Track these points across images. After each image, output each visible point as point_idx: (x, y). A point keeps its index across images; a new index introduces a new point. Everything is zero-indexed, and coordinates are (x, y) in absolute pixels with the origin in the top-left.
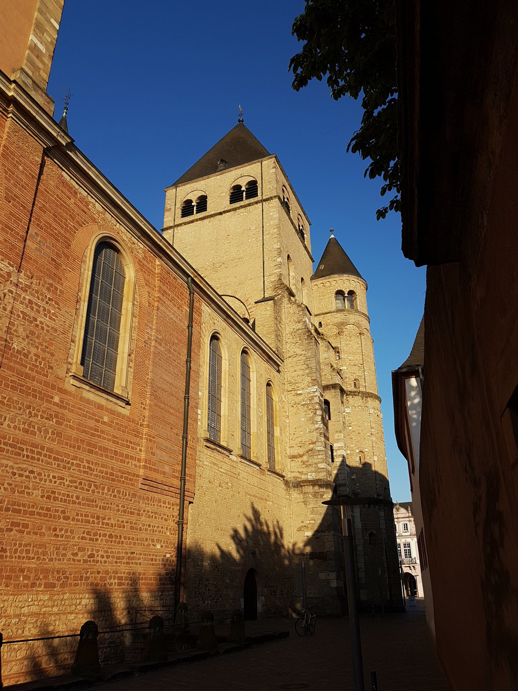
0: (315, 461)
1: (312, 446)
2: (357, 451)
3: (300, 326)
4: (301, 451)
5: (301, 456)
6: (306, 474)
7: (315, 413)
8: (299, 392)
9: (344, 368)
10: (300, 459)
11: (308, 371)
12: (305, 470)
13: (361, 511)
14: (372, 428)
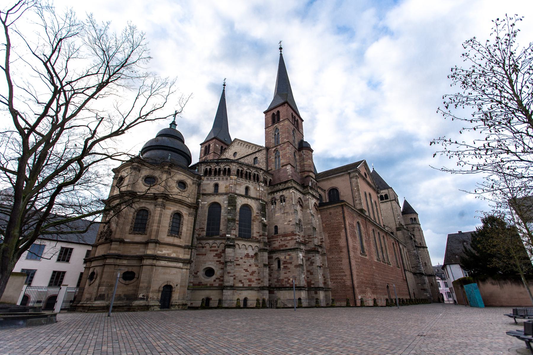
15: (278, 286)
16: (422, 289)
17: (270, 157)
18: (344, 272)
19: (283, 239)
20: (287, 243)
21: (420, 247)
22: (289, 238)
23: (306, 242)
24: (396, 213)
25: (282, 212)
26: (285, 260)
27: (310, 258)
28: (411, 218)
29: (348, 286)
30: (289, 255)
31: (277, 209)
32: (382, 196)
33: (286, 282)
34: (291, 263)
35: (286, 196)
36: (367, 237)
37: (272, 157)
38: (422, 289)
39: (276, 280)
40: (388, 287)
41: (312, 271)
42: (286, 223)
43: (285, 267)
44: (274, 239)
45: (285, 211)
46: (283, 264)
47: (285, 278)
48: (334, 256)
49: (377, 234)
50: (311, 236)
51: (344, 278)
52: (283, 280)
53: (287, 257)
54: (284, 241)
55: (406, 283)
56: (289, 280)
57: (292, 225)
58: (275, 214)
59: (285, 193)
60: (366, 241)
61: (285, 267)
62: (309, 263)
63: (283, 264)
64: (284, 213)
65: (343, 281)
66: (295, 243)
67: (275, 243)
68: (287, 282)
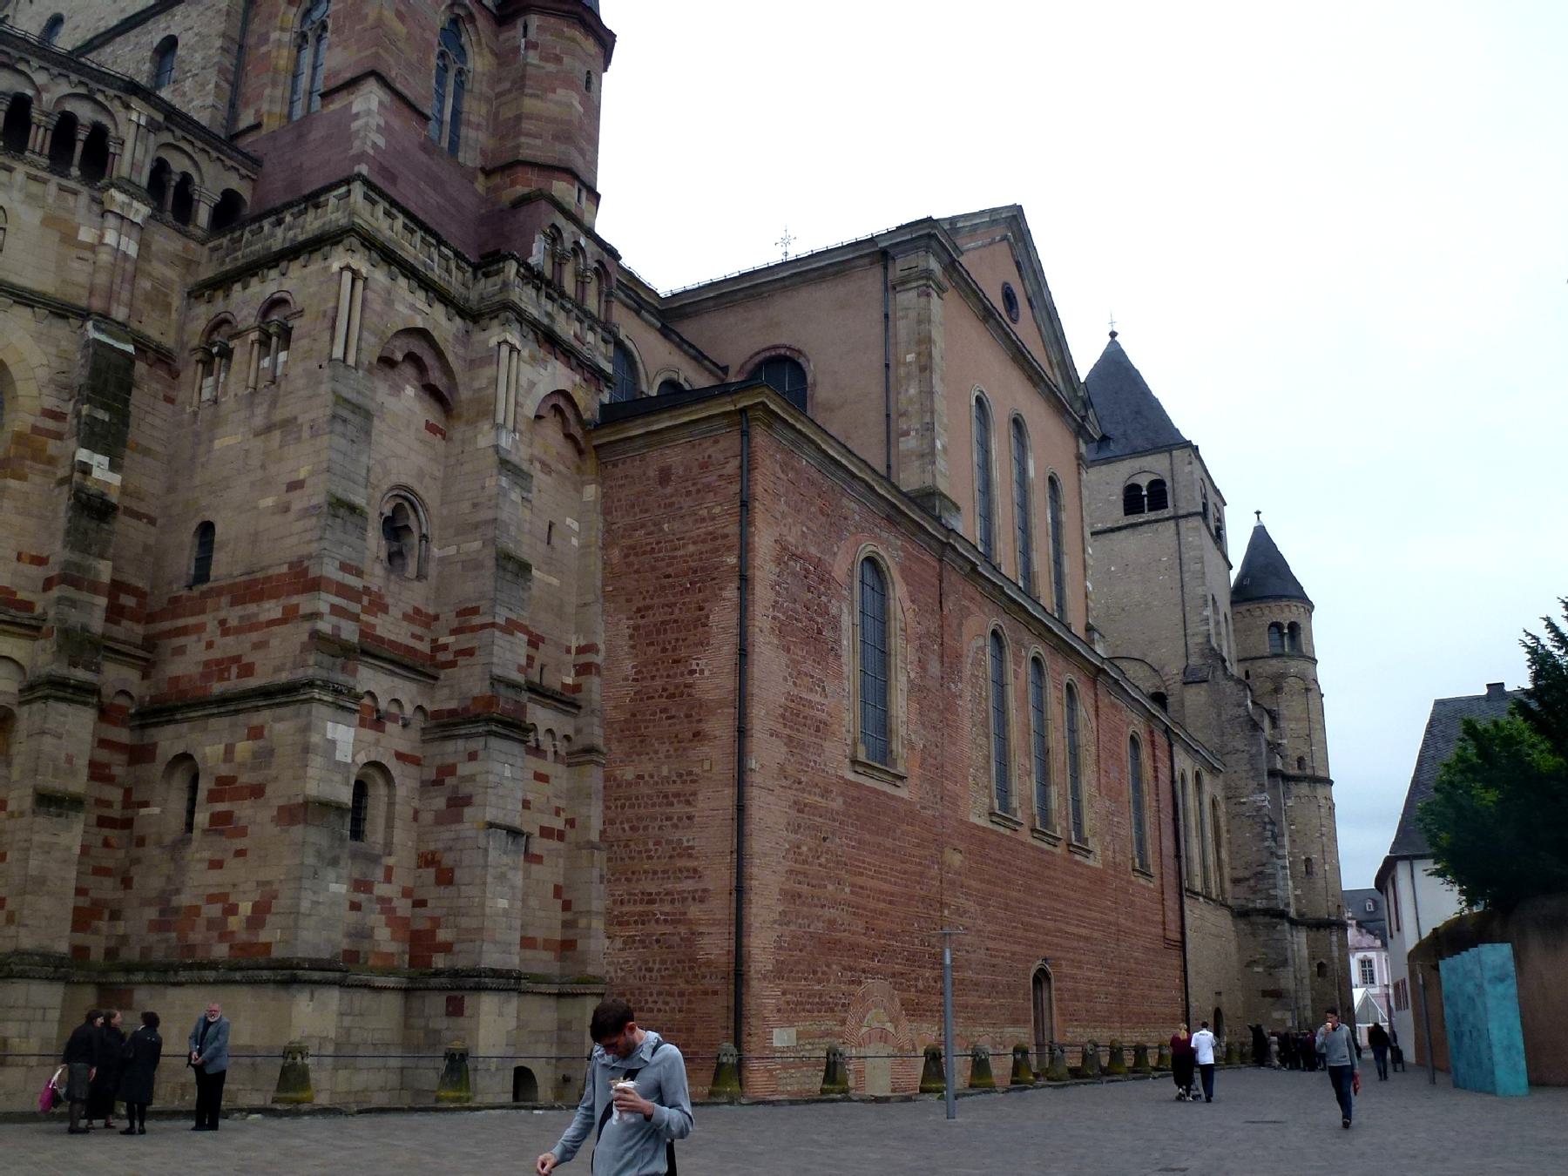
3: (1241, 711)
4: (1247, 874)
5: (1247, 879)
6: (1254, 901)
9: (1285, 741)
12: (1251, 897)
15: (158, 955)
16: (1265, 994)
17: (264, 39)
18: (695, 873)
19: (234, 616)
20: (257, 646)
21: (1296, 779)
22: (271, 609)
23: (442, 657)
24: (1195, 590)
25: (259, 421)
26: (224, 770)
27: (449, 770)
28: (1277, 626)
29: (709, 964)
30: (256, 733)
31: (228, 402)
32: (1139, 488)
33: (211, 924)
34: (257, 791)
35: (298, 300)
36: (935, 668)
37: (275, 35)
38: (1265, 994)
39: (152, 913)
40: (1041, 978)
41: (447, 860)
42: (269, 502)
43: (222, 822)
44: (181, 622)
45: (279, 415)
46: (214, 797)
47: (212, 899)
48: (647, 767)
50: (475, 611)
51: (694, 911)
52: (195, 911)
53: (244, 748)
54: (238, 631)
55: (1177, 962)
56: (232, 910)
57: (306, 513)
58: (211, 441)
59: (296, 281)
60: (917, 690)
61: (222, 822)
62: (440, 803)
63: (214, 797)
64: (269, 429)
65: (683, 930)
66: (304, 648)
67: (181, 651)
68: (219, 928)
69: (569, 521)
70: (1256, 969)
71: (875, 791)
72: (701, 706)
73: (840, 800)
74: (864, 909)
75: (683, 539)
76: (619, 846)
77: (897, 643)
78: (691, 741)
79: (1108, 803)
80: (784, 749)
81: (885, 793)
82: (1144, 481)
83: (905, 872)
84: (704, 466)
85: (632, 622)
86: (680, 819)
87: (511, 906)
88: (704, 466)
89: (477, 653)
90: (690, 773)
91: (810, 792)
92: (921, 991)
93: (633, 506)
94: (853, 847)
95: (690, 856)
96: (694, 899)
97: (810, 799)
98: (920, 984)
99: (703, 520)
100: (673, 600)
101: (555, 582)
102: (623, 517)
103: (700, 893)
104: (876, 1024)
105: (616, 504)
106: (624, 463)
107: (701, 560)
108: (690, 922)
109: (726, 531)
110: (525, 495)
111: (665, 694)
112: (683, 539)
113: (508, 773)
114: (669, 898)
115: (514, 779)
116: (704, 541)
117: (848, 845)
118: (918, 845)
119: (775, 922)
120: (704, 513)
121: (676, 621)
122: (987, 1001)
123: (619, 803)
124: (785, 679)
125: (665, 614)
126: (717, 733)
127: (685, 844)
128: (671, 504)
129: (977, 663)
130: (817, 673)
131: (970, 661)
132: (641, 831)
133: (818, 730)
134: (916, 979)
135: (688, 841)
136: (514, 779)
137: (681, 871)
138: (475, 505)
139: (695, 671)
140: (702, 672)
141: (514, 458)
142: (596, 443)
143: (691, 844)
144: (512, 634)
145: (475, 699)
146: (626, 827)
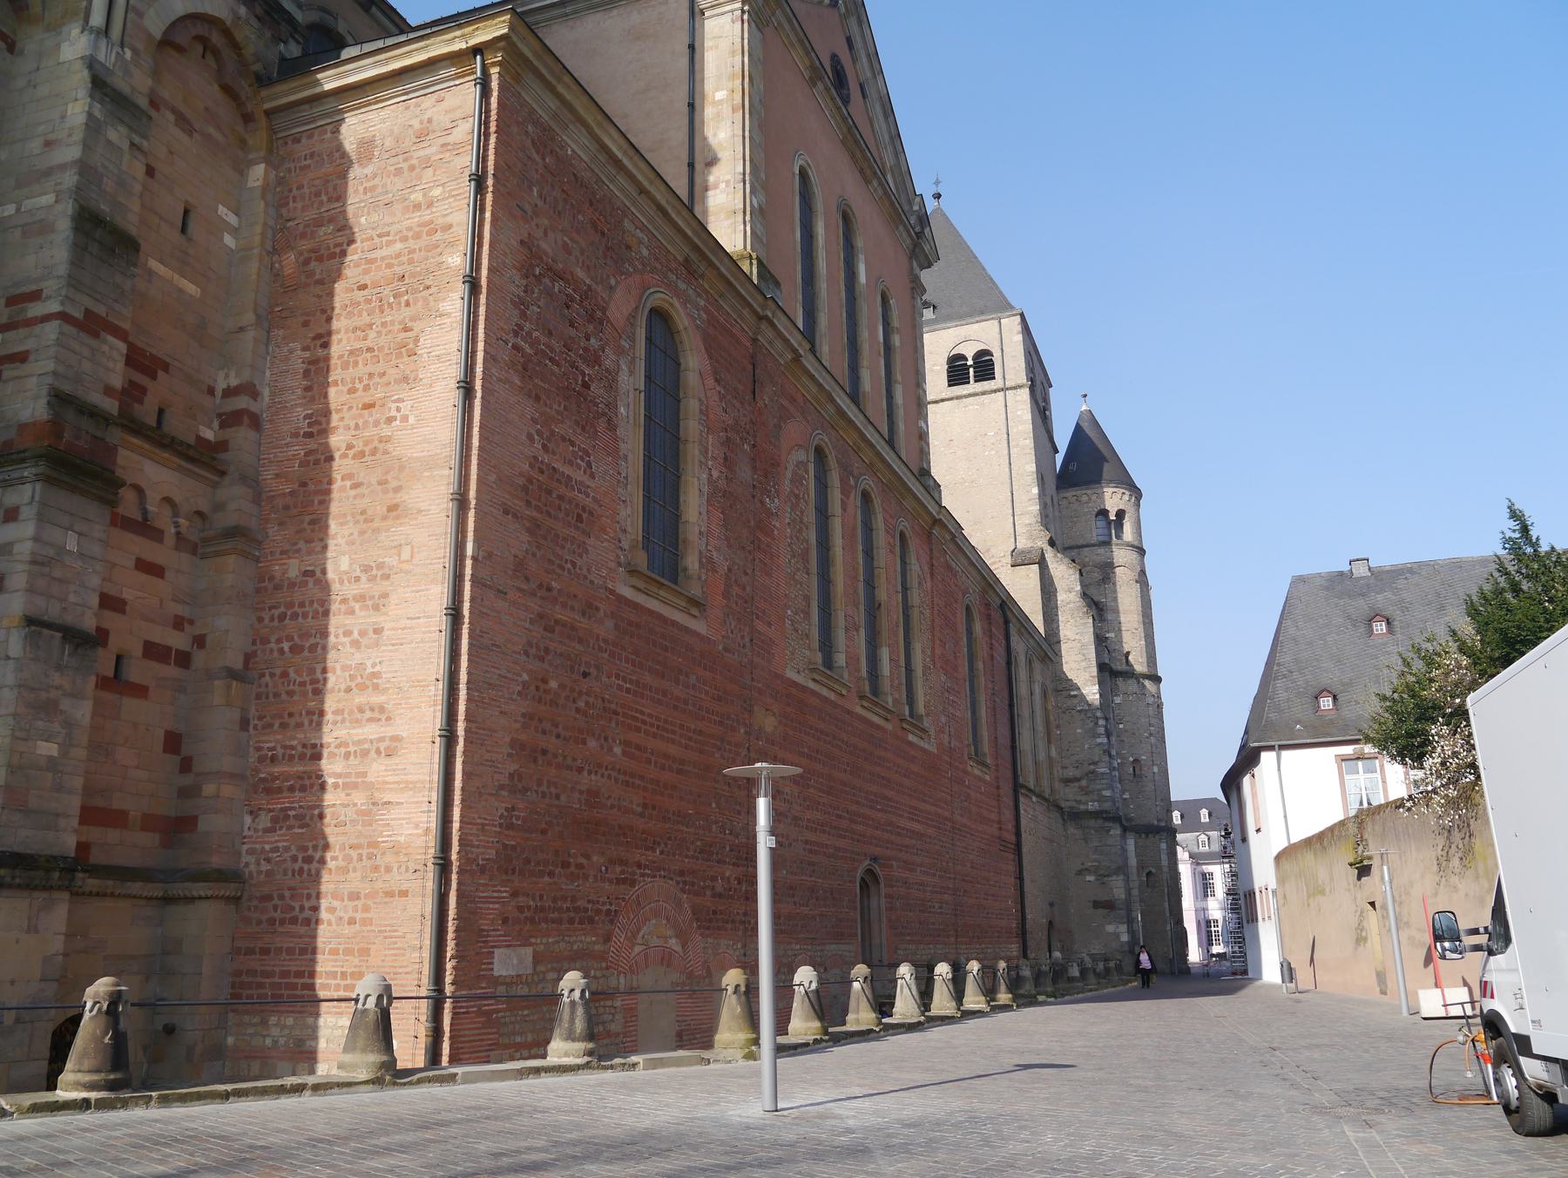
0: (1098, 787)
1: (1092, 767)
2: (1131, 759)
4: (1078, 773)
5: (1078, 780)
6: (1086, 803)
7: (1097, 724)
8: (1072, 693)
10: (1077, 784)
11: (1084, 664)
12: (1083, 798)
13: (1136, 843)
14: (1150, 725)
16: (1097, 904)
18: (380, 713)
29: (396, 849)
36: (745, 473)
38: (1097, 904)
40: (869, 881)
49: (855, 500)
55: (1011, 867)
60: (722, 498)
69: (222, 210)
70: (1088, 878)
71: (660, 617)
72: (402, 468)
73: (610, 624)
74: (642, 778)
75: (388, 234)
76: (272, 675)
77: (692, 426)
78: (384, 518)
79: (943, 678)
80: (525, 537)
81: (674, 623)
82: (969, 351)
83: (700, 733)
84: (422, 136)
85: (307, 354)
86: (363, 633)
87: (64, 754)
88: (422, 136)
89: (32, 358)
90: (380, 566)
91: (564, 605)
92: (720, 895)
93: (318, 194)
94: (628, 691)
95: (376, 687)
96: (378, 752)
97: (560, 614)
98: (719, 883)
99: (417, 207)
100: (366, 319)
101: (191, 289)
102: (304, 209)
103: (387, 743)
104: (655, 941)
105: (295, 192)
106: (310, 137)
107: (411, 262)
108: (369, 786)
109: (449, 219)
110: (137, 140)
111: (351, 453)
112: (388, 234)
113: (72, 544)
114: (343, 750)
115: (81, 555)
116: (417, 236)
117: (620, 688)
118: (720, 699)
119: (502, 787)
120: (416, 197)
121: (370, 350)
122: (805, 910)
123: (276, 612)
124: (530, 438)
125: (357, 339)
126: (423, 506)
127: (370, 670)
128: (373, 189)
129: (797, 480)
130: (581, 440)
131: (789, 474)
132: (306, 653)
133: (579, 519)
134: (714, 879)
135: (374, 665)
136: (81, 555)
137: (361, 710)
138: (48, 144)
139: (395, 418)
140: (405, 418)
141: (119, 82)
142: (267, 106)
143: (377, 668)
144: (96, 335)
145: (22, 427)
146: (286, 646)
